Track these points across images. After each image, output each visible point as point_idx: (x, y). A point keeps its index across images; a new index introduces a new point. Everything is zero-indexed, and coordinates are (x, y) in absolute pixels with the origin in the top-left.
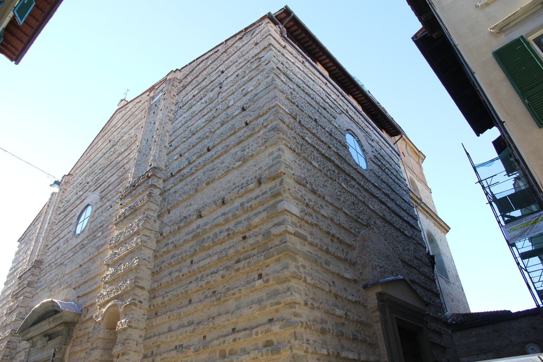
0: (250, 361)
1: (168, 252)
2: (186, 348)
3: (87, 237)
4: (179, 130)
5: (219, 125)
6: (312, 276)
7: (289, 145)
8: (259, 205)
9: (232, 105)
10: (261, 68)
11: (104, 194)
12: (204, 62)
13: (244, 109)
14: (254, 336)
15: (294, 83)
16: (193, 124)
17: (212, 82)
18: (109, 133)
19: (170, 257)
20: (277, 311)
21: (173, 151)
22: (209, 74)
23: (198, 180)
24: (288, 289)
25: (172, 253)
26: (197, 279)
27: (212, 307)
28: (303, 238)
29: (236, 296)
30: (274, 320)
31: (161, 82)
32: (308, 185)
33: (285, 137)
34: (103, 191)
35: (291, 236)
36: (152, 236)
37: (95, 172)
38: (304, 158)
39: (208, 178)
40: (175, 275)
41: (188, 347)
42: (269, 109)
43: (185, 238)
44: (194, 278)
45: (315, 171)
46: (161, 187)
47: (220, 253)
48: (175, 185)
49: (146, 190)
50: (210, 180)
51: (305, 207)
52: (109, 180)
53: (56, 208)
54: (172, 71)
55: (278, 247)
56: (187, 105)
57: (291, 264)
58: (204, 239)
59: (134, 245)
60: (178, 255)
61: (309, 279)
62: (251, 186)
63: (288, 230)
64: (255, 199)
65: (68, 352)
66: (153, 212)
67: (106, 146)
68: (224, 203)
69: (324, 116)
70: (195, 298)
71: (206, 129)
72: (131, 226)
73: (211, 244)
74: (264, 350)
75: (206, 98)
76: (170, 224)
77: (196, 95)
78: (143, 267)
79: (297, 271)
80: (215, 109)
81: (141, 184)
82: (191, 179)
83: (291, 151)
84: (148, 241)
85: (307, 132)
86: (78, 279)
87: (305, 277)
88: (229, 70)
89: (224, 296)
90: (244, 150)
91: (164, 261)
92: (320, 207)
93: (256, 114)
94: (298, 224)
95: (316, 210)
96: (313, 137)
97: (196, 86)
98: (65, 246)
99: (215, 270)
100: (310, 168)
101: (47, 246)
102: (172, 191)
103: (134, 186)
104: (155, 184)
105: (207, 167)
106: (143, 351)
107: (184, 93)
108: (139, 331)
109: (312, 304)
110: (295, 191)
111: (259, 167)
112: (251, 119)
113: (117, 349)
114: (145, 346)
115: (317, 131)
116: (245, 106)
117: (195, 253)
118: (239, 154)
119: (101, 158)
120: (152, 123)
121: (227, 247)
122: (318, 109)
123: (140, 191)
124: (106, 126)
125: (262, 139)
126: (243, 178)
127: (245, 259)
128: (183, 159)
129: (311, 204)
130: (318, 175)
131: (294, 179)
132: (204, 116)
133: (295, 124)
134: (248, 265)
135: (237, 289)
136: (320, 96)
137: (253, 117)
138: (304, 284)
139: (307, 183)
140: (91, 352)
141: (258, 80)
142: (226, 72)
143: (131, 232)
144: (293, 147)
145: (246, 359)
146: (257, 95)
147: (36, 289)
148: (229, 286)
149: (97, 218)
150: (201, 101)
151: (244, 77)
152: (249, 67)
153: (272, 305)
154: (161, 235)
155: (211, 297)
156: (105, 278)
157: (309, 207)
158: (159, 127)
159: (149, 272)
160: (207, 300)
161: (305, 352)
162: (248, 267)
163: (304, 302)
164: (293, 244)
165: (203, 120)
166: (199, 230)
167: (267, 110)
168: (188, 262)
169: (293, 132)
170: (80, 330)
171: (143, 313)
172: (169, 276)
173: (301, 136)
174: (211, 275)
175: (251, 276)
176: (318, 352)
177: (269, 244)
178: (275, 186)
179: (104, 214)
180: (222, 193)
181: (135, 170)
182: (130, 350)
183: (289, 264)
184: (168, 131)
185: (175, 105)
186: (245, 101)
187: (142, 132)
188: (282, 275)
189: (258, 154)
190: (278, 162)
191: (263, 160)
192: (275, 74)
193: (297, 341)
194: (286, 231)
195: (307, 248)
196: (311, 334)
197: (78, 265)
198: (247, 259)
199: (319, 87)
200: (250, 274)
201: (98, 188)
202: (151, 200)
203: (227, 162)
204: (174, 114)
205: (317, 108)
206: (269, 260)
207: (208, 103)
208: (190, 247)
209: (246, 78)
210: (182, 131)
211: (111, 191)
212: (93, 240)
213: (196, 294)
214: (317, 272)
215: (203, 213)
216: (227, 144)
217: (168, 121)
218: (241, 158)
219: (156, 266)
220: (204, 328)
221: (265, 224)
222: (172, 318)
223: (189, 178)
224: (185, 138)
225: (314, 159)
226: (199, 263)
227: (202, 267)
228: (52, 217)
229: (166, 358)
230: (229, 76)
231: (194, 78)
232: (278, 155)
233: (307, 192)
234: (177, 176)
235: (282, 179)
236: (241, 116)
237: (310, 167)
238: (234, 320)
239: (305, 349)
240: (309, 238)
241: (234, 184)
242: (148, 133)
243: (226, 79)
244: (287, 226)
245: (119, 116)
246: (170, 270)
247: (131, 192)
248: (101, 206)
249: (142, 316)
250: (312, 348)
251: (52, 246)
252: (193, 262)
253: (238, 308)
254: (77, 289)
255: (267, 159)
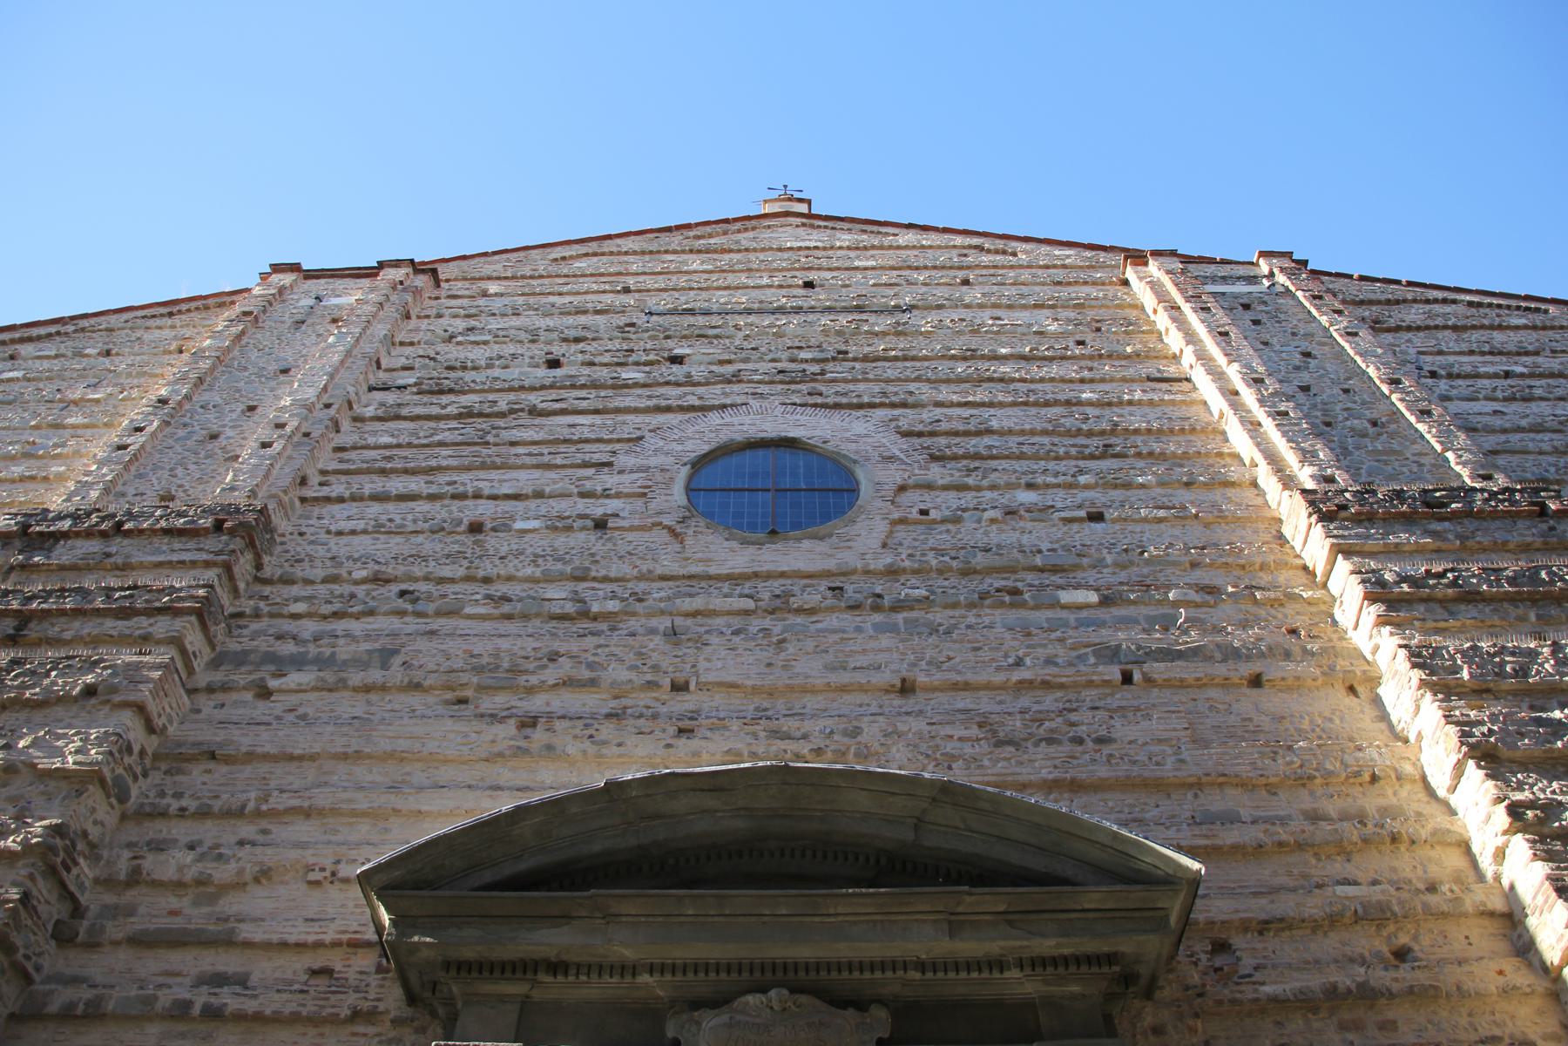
98: (561, 541)
147: (240, 659)
197: (888, 677)
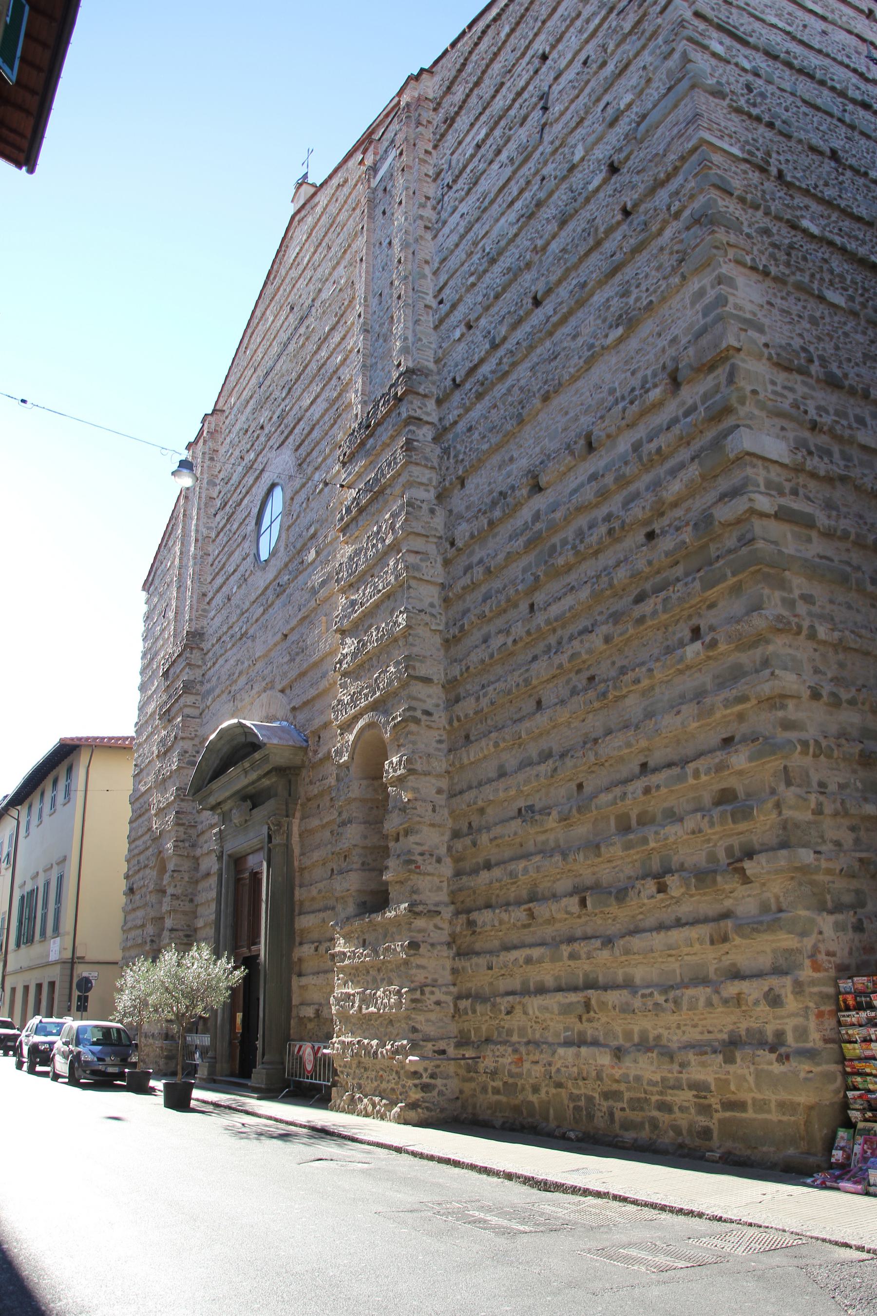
0: (685, 837)
1: (474, 586)
2: (541, 812)
3: (286, 565)
4: (456, 253)
5: (553, 226)
6: (832, 619)
7: (748, 259)
8: (679, 446)
9: (582, 159)
10: (648, 27)
11: (304, 454)
12: (491, 32)
13: (613, 169)
14: (691, 781)
15: (756, 48)
16: (487, 233)
17: (519, 94)
18: (287, 286)
19: (480, 599)
20: (741, 717)
21: (447, 315)
22: (510, 71)
23: (521, 389)
24: (766, 663)
25: (484, 589)
26: (549, 648)
27: (591, 716)
28: (808, 523)
29: (642, 685)
30: (737, 739)
31: (387, 115)
32: (815, 368)
33: (733, 238)
34: (300, 445)
35: (765, 522)
36: (432, 549)
37: (273, 396)
38: (800, 287)
39: (546, 383)
40: (496, 642)
41: (546, 811)
42: (683, 159)
43: (508, 549)
44: (541, 646)
45: (836, 319)
46: (434, 418)
47: (594, 580)
48: (467, 410)
49: (398, 434)
50: (551, 388)
51: (807, 434)
52: (308, 414)
53: (203, 500)
54: (411, 78)
55: (732, 557)
56: (465, 175)
57: (769, 598)
58: (554, 547)
59: (392, 578)
60: (498, 591)
61: (822, 631)
62: (655, 394)
63: (758, 506)
64: (668, 428)
65: (295, 830)
66: (422, 488)
67: (286, 324)
68: (590, 447)
69: (862, 133)
70: (549, 696)
71: (523, 242)
72: (378, 532)
73: (572, 560)
74: (716, 812)
75: (512, 146)
76: (469, 515)
77: (484, 141)
78: (421, 631)
79: (786, 613)
80: (538, 178)
81: (384, 417)
82: (504, 391)
83: (755, 276)
84: (424, 564)
85: (807, 201)
86: (286, 667)
87: (812, 627)
88: (560, 47)
89: (615, 688)
90: (625, 294)
91: (468, 610)
92: (855, 425)
93: (647, 178)
94: (788, 486)
95: (842, 437)
96: (826, 213)
97: (481, 114)
98: (243, 591)
99: (588, 623)
100: (818, 314)
101: (204, 595)
102: (461, 427)
103: (368, 426)
104: (416, 415)
105: (539, 351)
106: (450, 823)
107: (451, 139)
108: (434, 781)
109: (833, 694)
110: (775, 393)
111: (669, 338)
112: (636, 196)
113: (393, 823)
114: (452, 813)
115: (840, 190)
116: (615, 158)
117: (536, 585)
118: (616, 304)
119: (279, 356)
120: (385, 244)
121: (611, 562)
122: (840, 115)
123: (385, 437)
124: (275, 267)
125: (671, 253)
126: (633, 374)
127: (657, 590)
128: (477, 335)
129: (826, 420)
130: (847, 328)
131: (770, 358)
132: (512, 203)
133: (766, 184)
134: (664, 606)
135: (644, 669)
136: (847, 67)
137: (641, 188)
138: (811, 645)
139: (811, 361)
140: (341, 830)
141: (644, 68)
142: (554, 55)
143: (380, 545)
144: (762, 261)
145: (676, 834)
146: (644, 117)
148: (625, 662)
149: (298, 517)
150: (498, 159)
151: (604, 64)
152: (616, 26)
153: (727, 704)
154: (452, 544)
155: (586, 690)
156: (340, 662)
157: (821, 431)
158: (402, 255)
159: (438, 640)
160: (575, 699)
161: (813, 813)
162: (665, 611)
163: (808, 692)
164: (772, 542)
165: (512, 216)
166: (538, 526)
167: (677, 164)
168: (524, 607)
169: (760, 214)
170: (311, 783)
171: (438, 738)
172: (484, 646)
173: (788, 221)
174: (579, 639)
175: (674, 633)
176: (853, 811)
177: (712, 547)
178: (716, 389)
179: (313, 504)
180: (585, 421)
181: (363, 382)
182: (420, 823)
183: (765, 599)
184: (427, 262)
185: (435, 180)
186: (614, 141)
187: (363, 275)
188: (746, 627)
189: (663, 300)
190: (720, 318)
191: (679, 314)
192: (690, 40)
193: (793, 788)
194: (752, 511)
195: (817, 547)
196: (832, 769)
197: (279, 636)
198: (661, 590)
199: (842, 36)
200: (670, 629)
201: (287, 438)
202: (413, 460)
203: (586, 331)
204: (434, 208)
205: (836, 112)
206: (715, 589)
207: (517, 164)
208: (524, 571)
209: (610, 68)
210: (464, 256)
211: (318, 443)
212: (301, 573)
213: (551, 685)
214: (849, 607)
215: (543, 480)
216: (582, 281)
217: (421, 231)
218: (620, 316)
219: (451, 623)
220: (575, 766)
221: (698, 497)
222: (502, 745)
223: (499, 387)
224: (472, 274)
225: (831, 283)
226: (549, 608)
227: (556, 620)
228: (201, 524)
229: (502, 837)
230: (562, 67)
231: (471, 90)
232: (716, 298)
233: (812, 388)
234: (468, 386)
235: (733, 366)
236: (609, 189)
237: (820, 310)
238: (643, 743)
239: (813, 805)
240: (822, 519)
241: (612, 391)
242: (378, 274)
243: (556, 78)
244: (753, 496)
245: (300, 235)
246: (485, 630)
247: (363, 444)
248: (303, 486)
249: (435, 745)
250: (834, 802)
251: (215, 595)
252: (536, 607)
253: (649, 715)
254: (288, 691)
255: (689, 313)
